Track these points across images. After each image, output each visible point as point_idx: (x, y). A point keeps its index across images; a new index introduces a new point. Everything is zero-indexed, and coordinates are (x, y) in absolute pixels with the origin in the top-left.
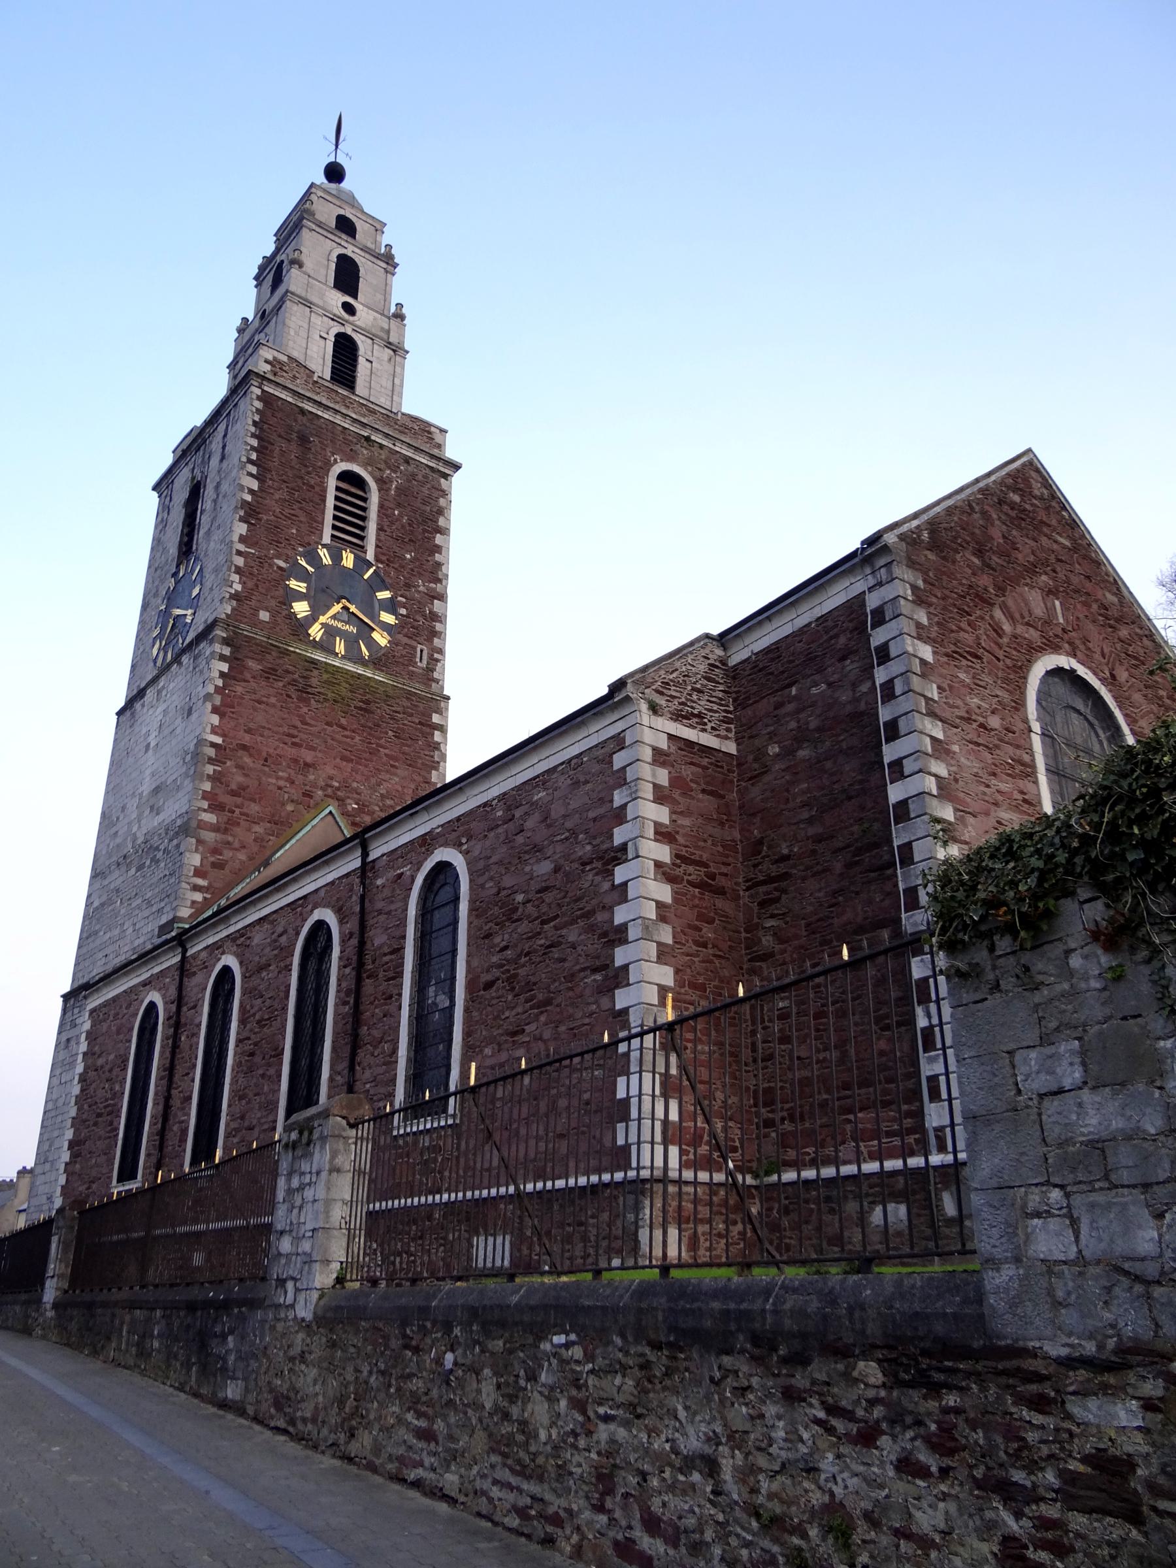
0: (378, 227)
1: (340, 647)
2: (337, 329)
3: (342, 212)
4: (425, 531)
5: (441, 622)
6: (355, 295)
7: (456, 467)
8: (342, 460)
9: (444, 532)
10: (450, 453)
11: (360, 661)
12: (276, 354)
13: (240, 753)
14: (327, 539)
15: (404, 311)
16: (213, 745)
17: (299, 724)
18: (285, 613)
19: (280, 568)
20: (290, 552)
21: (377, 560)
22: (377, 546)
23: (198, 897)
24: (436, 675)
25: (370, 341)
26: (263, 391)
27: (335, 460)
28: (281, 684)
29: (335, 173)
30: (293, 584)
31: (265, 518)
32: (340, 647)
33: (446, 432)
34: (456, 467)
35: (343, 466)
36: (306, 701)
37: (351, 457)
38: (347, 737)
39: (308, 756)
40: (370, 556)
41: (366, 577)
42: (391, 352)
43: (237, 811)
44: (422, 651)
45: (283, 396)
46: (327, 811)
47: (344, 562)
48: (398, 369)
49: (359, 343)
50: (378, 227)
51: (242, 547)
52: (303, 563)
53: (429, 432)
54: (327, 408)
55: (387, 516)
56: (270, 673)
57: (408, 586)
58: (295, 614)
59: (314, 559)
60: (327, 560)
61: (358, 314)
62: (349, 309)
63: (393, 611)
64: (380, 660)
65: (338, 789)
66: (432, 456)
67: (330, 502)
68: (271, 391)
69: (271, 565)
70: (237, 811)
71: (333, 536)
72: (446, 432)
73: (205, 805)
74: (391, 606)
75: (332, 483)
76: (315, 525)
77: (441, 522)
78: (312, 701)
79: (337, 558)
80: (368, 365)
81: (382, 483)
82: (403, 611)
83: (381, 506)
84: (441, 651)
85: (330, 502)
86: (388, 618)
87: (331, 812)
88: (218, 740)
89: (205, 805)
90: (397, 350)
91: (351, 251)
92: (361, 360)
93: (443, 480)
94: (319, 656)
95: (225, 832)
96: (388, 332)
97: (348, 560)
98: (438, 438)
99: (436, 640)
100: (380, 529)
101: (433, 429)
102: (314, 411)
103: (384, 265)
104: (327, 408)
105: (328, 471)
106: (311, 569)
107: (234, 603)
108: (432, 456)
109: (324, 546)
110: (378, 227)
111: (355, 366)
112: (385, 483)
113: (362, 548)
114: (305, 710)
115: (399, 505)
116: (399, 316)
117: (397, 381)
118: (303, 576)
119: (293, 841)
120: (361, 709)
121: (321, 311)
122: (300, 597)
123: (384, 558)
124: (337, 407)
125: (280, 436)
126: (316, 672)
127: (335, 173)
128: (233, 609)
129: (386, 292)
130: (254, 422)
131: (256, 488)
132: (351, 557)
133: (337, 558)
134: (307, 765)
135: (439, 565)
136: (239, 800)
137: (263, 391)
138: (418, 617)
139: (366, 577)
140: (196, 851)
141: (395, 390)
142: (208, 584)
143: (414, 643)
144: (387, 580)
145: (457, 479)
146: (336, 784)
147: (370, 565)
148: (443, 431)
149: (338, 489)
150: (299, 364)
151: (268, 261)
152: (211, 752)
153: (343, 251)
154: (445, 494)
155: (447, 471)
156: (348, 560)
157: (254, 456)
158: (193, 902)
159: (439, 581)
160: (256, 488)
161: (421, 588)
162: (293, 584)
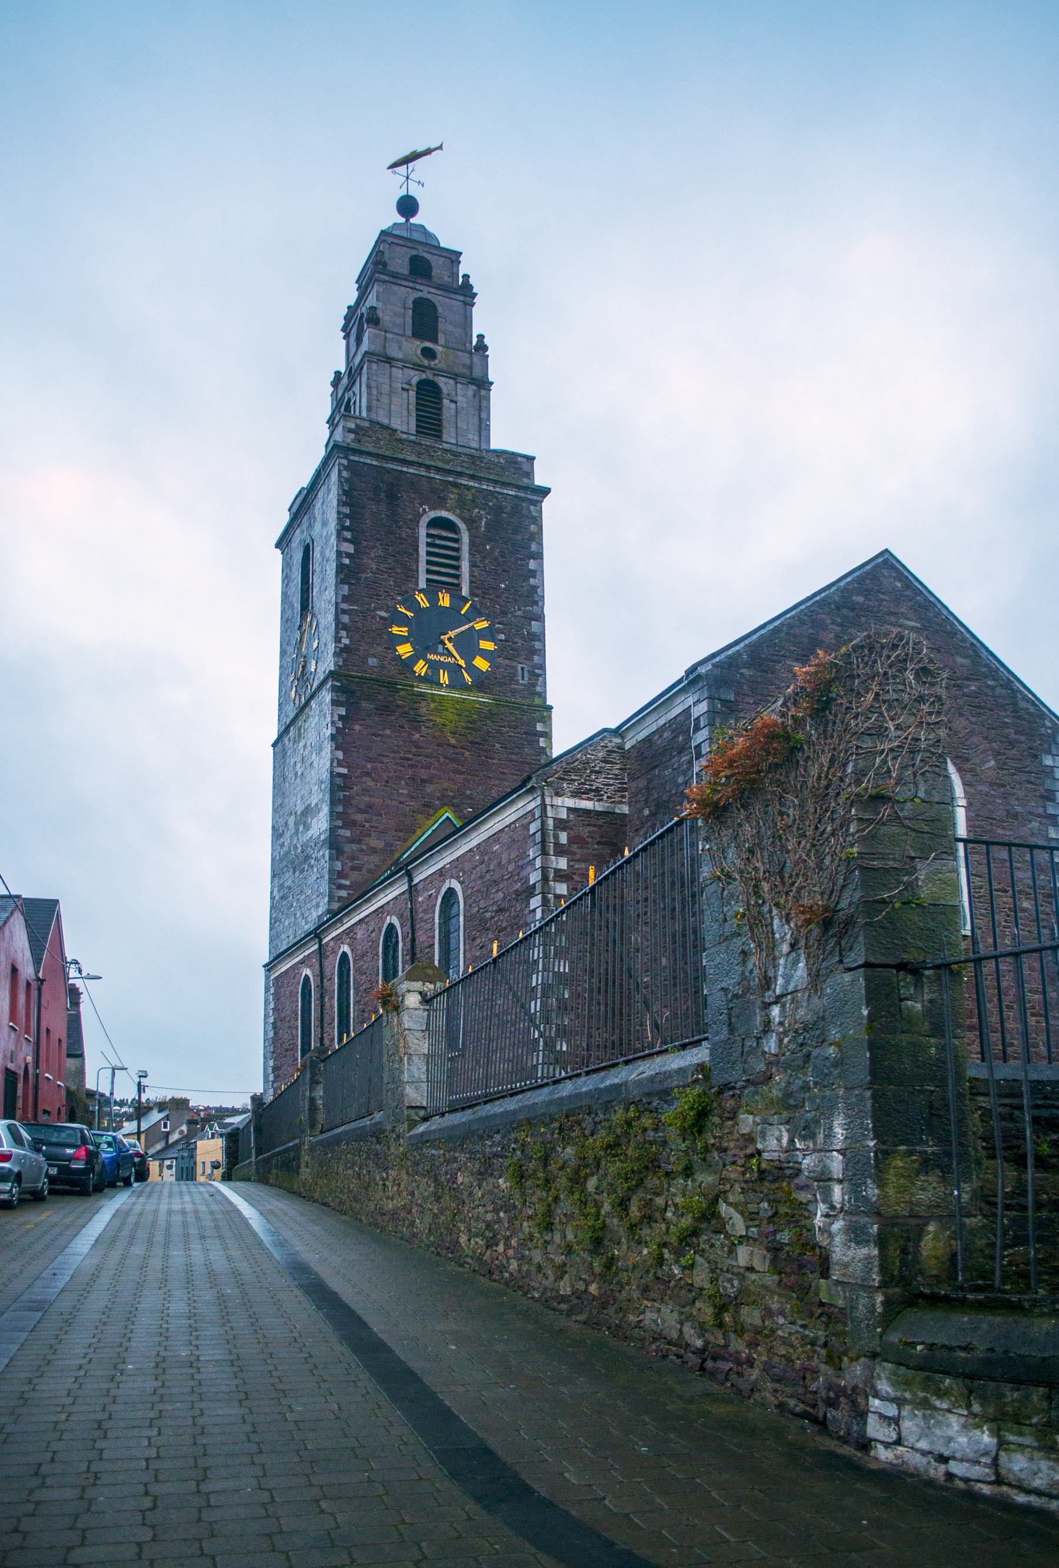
0: (454, 257)
1: (444, 678)
2: (416, 377)
3: (415, 252)
4: (518, 559)
5: (540, 640)
6: (435, 341)
7: (545, 492)
8: (430, 509)
9: (539, 556)
10: (539, 480)
11: (466, 688)
12: (358, 421)
13: (365, 779)
14: (422, 585)
15: (486, 341)
16: (340, 775)
17: (414, 750)
18: (390, 656)
19: (382, 618)
20: (390, 603)
21: (472, 594)
22: (471, 582)
23: (343, 893)
24: (538, 689)
25: (452, 382)
26: (349, 461)
27: (424, 510)
28: (393, 718)
29: (408, 206)
30: (395, 630)
31: (363, 576)
32: (444, 678)
33: (534, 458)
34: (545, 492)
35: (433, 514)
36: (418, 729)
37: (441, 503)
38: (457, 754)
39: (424, 774)
40: (465, 591)
41: (463, 612)
42: (475, 388)
43: (367, 825)
44: (522, 669)
45: (369, 461)
46: (444, 817)
47: (441, 603)
48: (484, 403)
49: (442, 385)
50: (454, 257)
51: (345, 606)
52: (403, 610)
53: (516, 463)
54: (411, 463)
55: (479, 552)
56: (385, 709)
57: (504, 613)
58: (400, 656)
59: (414, 605)
60: (424, 604)
61: (439, 356)
62: (429, 353)
63: (492, 639)
64: (482, 683)
65: (453, 798)
66: (519, 488)
67: (423, 550)
68: (356, 459)
69: (374, 617)
70: (367, 825)
71: (428, 580)
72: (534, 458)
73: (340, 823)
74: (489, 634)
75: (423, 531)
76: (410, 573)
77: (534, 547)
78: (423, 728)
79: (433, 599)
80: (453, 406)
81: (472, 523)
82: (502, 637)
83: (472, 544)
84: (542, 667)
85: (423, 550)
86: (487, 645)
87: (448, 818)
88: (345, 771)
89: (340, 823)
90: (483, 384)
91: (425, 292)
92: (446, 402)
93: (532, 508)
94: (424, 689)
95: (359, 842)
96: (470, 367)
97: (445, 601)
98: (526, 467)
99: (536, 658)
100: (473, 565)
101: (519, 459)
102: (400, 468)
103: (461, 298)
104: (411, 463)
105: (418, 522)
106: (409, 614)
107: (345, 655)
108: (519, 488)
109: (420, 591)
110: (453, 257)
111: (440, 409)
112: (474, 521)
113: (458, 586)
114: (418, 736)
115: (490, 540)
116: (482, 347)
117: (484, 416)
118: (403, 621)
119: (418, 844)
120: (467, 728)
121: (400, 364)
122: (403, 640)
123: (479, 592)
124: (420, 461)
125: (369, 499)
126: (424, 704)
127: (408, 206)
128: (345, 661)
129: (467, 323)
130: (344, 491)
131: (352, 551)
133: (433, 599)
134: (423, 781)
135: (534, 588)
136: (367, 816)
137: (349, 461)
138: (516, 640)
139: (463, 612)
140: (337, 859)
141: (483, 427)
142: (323, 640)
143: (514, 664)
144: (484, 611)
145: (547, 504)
146: (451, 794)
147: (465, 600)
148: (531, 459)
149: (429, 535)
150: (383, 427)
151: (352, 310)
152: (339, 781)
153: (419, 294)
154: (537, 521)
155: (535, 498)
157: (348, 523)
158: (340, 898)
159: (536, 603)
160: (352, 551)
161: (519, 613)
162: (395, 630)
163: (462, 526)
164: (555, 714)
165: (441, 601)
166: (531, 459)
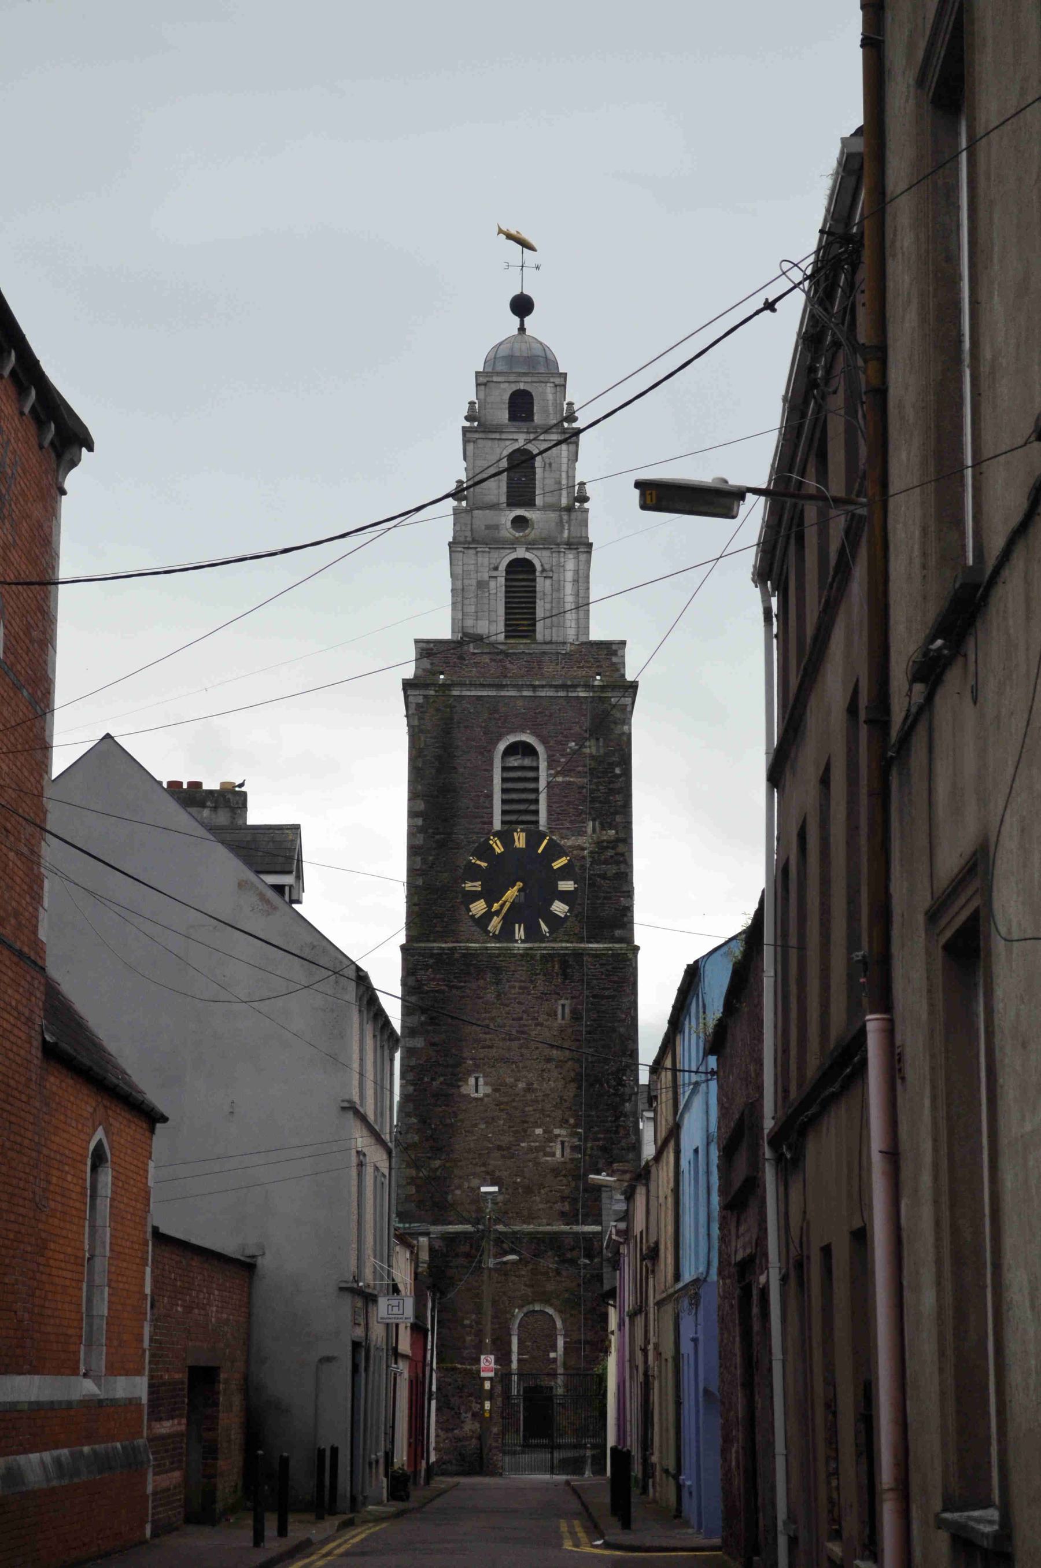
14: (497, 826)
15: (589, 490)
29: (522, 306)
41: (540, 851)
59: (485, 851)
60: (499, 849)
62: (520, 522)
86: (566, 886)
97: (520, 840)
106: (484, 864)
113: (537, 822)
116: (584, 499)
127: (522, 306)
132: (523, 835)
139: (540, 851)
148: (623, 643)
156: (520, 840)
163: (540, 749)
164: (641, 956)
165: (517, 843)
166: (623, 643)
